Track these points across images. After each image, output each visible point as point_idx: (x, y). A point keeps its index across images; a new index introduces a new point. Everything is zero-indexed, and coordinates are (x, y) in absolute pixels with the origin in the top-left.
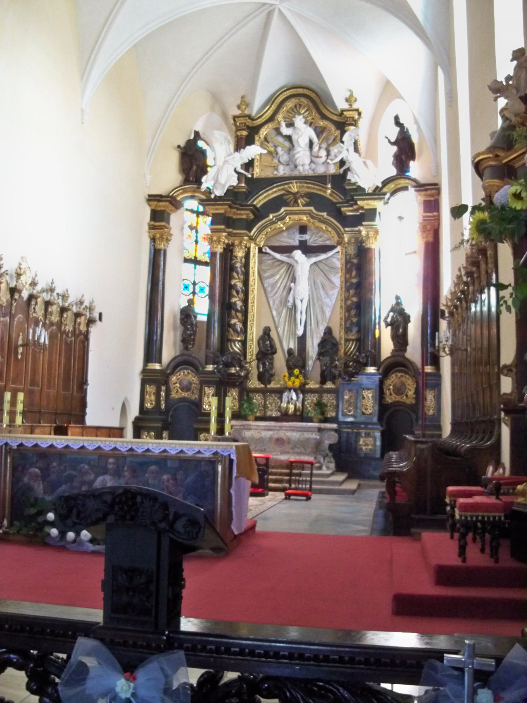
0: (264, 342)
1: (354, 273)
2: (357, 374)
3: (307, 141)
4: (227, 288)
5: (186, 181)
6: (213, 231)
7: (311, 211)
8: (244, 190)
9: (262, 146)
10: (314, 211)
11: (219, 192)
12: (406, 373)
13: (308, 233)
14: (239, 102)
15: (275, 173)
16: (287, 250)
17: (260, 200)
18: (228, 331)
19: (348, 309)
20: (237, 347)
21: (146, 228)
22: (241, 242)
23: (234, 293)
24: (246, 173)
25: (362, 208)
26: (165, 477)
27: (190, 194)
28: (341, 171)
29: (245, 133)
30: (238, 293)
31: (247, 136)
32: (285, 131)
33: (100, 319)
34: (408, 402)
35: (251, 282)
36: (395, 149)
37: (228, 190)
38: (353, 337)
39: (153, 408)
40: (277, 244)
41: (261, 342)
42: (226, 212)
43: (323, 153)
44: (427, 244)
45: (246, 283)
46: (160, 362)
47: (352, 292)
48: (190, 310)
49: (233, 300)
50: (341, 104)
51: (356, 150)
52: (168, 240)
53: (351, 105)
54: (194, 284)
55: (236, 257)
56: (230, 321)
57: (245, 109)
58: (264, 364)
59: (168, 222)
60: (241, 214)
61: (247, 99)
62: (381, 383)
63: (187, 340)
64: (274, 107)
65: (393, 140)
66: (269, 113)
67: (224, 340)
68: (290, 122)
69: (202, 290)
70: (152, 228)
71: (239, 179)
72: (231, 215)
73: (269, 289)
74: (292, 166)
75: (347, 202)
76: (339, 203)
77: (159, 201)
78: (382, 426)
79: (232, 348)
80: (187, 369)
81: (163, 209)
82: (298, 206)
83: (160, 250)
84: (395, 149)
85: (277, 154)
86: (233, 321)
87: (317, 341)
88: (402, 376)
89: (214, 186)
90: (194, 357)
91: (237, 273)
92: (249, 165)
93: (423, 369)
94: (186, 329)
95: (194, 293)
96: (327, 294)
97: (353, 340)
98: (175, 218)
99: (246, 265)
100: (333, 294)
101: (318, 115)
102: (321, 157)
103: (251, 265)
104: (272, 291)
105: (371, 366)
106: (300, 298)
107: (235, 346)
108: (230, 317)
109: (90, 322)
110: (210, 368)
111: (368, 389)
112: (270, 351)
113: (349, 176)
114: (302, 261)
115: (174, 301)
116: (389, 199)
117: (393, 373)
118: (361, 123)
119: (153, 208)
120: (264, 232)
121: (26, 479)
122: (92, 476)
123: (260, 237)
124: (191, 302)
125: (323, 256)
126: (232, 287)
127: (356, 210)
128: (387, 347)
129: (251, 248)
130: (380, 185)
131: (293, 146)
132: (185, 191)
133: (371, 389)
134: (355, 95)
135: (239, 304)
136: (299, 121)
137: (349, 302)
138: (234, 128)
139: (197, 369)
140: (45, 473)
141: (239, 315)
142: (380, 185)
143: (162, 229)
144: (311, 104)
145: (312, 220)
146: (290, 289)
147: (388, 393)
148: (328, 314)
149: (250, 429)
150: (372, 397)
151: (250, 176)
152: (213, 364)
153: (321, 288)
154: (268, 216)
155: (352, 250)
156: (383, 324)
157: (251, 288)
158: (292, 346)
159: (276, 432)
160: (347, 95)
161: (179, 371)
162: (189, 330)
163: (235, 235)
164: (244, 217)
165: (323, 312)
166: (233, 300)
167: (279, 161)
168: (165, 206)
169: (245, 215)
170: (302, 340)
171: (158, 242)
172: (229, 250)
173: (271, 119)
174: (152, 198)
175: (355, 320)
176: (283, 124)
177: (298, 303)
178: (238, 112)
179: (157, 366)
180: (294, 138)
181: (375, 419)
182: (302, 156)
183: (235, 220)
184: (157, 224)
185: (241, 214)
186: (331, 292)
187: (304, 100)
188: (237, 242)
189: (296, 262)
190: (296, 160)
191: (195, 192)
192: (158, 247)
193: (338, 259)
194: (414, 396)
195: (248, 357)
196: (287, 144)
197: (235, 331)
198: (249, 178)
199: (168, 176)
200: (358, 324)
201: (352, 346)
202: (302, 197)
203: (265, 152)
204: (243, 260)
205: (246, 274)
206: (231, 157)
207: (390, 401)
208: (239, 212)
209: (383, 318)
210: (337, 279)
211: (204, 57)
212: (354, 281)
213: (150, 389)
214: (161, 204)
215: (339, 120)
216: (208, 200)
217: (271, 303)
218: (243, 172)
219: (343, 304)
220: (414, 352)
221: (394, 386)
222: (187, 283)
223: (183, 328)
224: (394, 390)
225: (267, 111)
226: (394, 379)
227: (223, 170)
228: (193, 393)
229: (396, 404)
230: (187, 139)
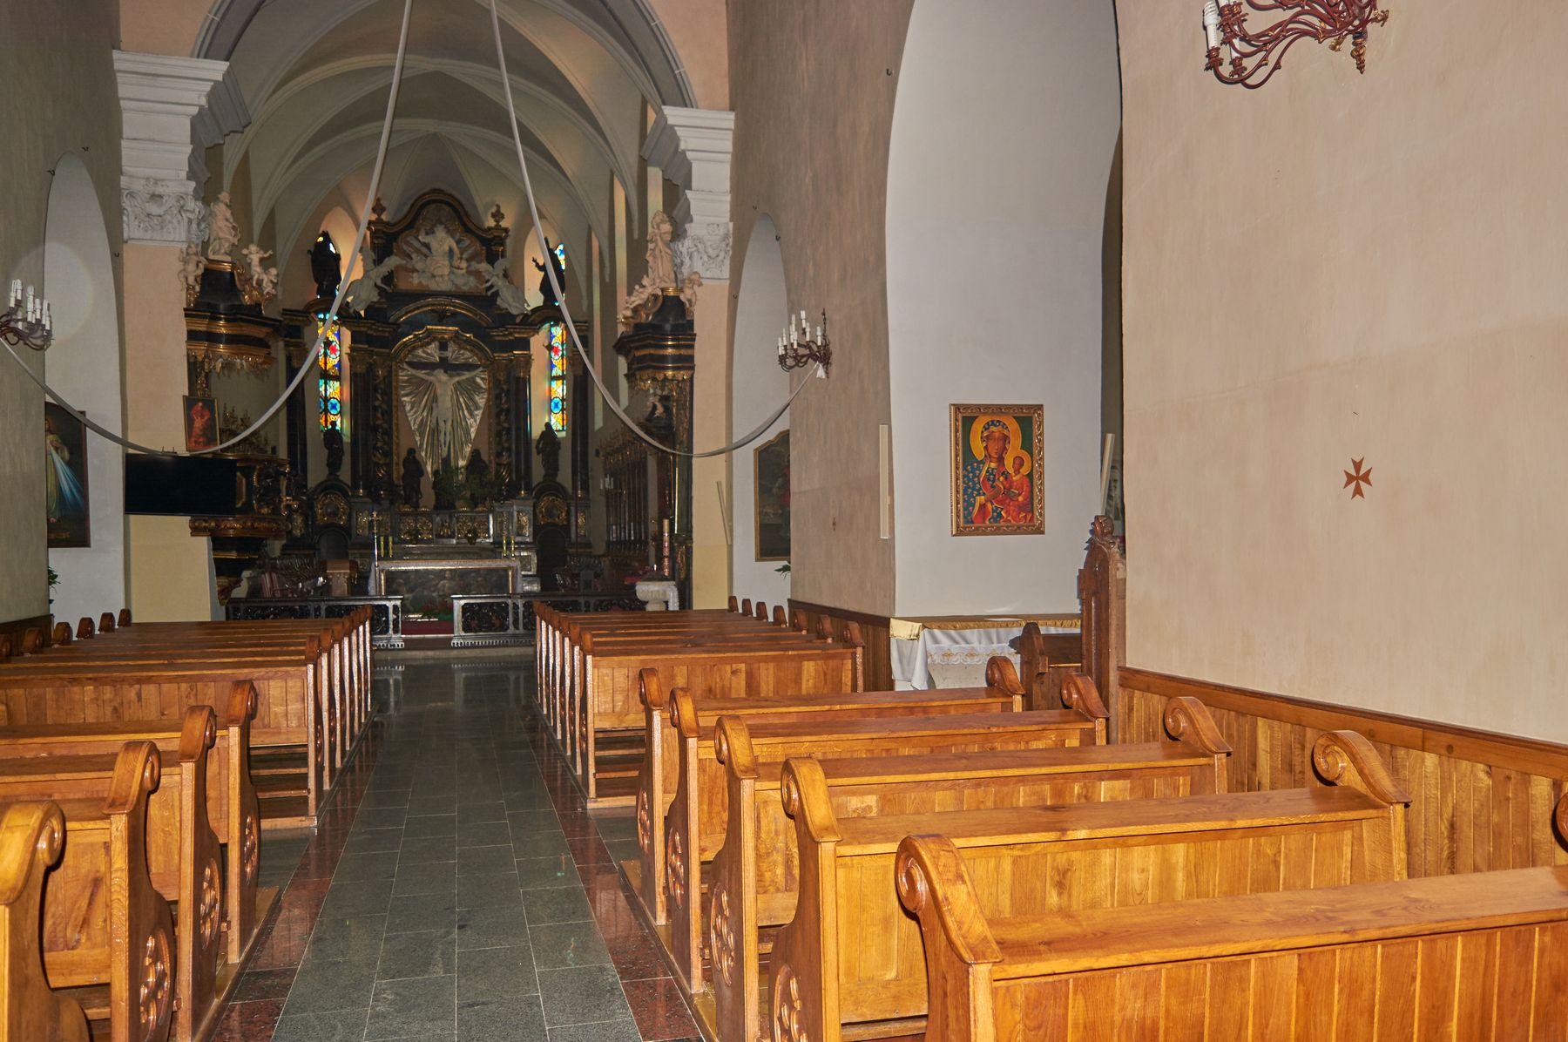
16: (431, 366)
43: (464, 265)
44: (575, 377)
45: (389, 402)
51: (505, 275)
63: (334, 463)
69: (334, 407)
92: (388, 279)
95: (326, 411)
96: (472, 415)
98: (307, 332)
113: (499, 301)
114: (444, 383)
115: (316, 425)
118: (508, 241)
125: (467, 375)
126: (376, 409)
136: (441, 233)
139: (345, 495)
160: (494, 210)
163: (378, 354)
165: (468, 433)
170: (446, 461)
172: (371, 368)
177: (441, 423)
178: (374, 217)
180: (434, 245)
187: (447, 209)
196: (424, 250)
210: (481, 400)
216: (346, 316)
220: (565, 477)
229: (547, 524)
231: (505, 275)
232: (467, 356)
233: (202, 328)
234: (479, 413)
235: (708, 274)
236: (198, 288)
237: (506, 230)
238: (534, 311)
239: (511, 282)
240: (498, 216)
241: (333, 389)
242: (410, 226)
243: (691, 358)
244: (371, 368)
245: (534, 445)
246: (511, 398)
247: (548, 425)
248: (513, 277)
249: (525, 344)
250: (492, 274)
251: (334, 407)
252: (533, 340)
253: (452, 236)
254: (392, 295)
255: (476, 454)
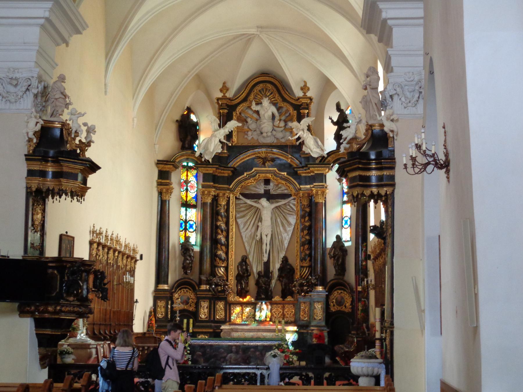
0: (242, 267)
1: (307, 219)
2: (311, 291)
3: (270, 114)
4: (215, 228)
5: (183, 148)
6: (203, 186)
7: (275, 171)
8: (226, 155)
9: (239, 120)
10: (277, 171)
11: (208, 157)
12: (345, 290)
13: (271, 184)
14: (221, 86)
15: (246, 136)
16: (257, 197)
17: (236, 162)
18: (215, 260)
19: (303, 244)
20: (221, 271)
21: (155, 184)
22: (224, 194)
23: (220, 231)
24: (228, 143)
25: (313, 172)
26: (257, 353)
27: (186, 157)
28: (298, 143)
29: (226, 111)
30: (222, 231)
31: (227, 113)
32: (254, 107)
33: (141, 258)
34: (347, 310)
35: (231, 223)
36: (336, 127)
37: (215, 156)
38: (306, 265)
39: (163, 318)
40: (247, 192)
41: (239, 267)
42: (214, 172)
43: (282, 124)
45: (227, 224)
46: (167, 284)
47: (306, 232)
48: (189, 245)
49: (219, 237)
50: (298, 93)
52: (171, 193)
53: (305, 93)
54: (186, 222)
55: (221, 205)
56: (217, 252)
57: (226, 92)
58: (241, 284)
59: (170, 180)
60: (224, 173)
61: (228, 85)
62: (327, 297)
64: (247, 91)
65: (335, 119)
66: (244, 95)
67: (214, 266)
68: (259, 102)
69: (191, 226)
70: (159, 184)
71: (222, 147)
72: (217, 174)
73: (241, 226)
74: (259, 132)
75: (303, 167)
76: (296, 168)
77: (166, 164)
78: (328, 328)
79: (219, 272)
80: (185, 288)
81: (168, 170)
82: (265, 167)
83: (165, 201)
84: (336, 127)
85: (247, 122)
86: (220, 252)
87: (278, 266)
88: (341, 293)
89: (205, 152)
90: (192, 280)
91: (222, 217)
92: (229, 136)
93: (357, 288)
94: (186, 259)
95: (186, 229)
96: (285, 230)
97: (307, 267)
99: (227, 211)
100: (290, 230)
101: (280, 98)
102: (281, 127)
103: (231, 210)
104: (244, 227)
105: (320, 286)
106: (265, 233)
107: (221, 270)
108: (216, 248)
109: (136, 261)
110: (204, 287)
111: (318, 302)
112: (246, 275)
113: (304, 149)
116: (332, 167)
117: (335, 291)
118: (313, 106)
119: (160, 169)
120: (240, 186)
121: (195, 357)
122: (226, 354)
123: (237, 189)
124: (187, 238)
125: (282, 202)
126: (217, 227)
127: (309, 173)
128: (331, 272)
129: (231, 198)
130: (326, 156)
131: (260, 117)
132: (182, 156)
133: (320, 302)
134: (308, 85)
135: (223, 240)
136: (266, 102)
137: (304, 240)
138: (217, 106)
139: (194, 289)
140: (204, 354)
141: (224, 248)
142: (326, 156)
143: (168, 185)
144: (275, 90)
145: (275, 178)
146: (258, 226)
147: (332, 304)
148: (286, 245)
149: (237, 332)
150: (321, 307)
151: (230, 145)
152: (206, 284)
153: (280, 225)
154: (244, 174)
155: (305, 202)
156: (328, 256)
157: (230, 228)
158: (259, 269)
159: (255, 333)
160: (302, 85)
161: (180, 289)
162: (188, 260)
164: (226, 175)
166: (219, 237)
167: (248, 128)
168: (169, 168)
169: (227, 173)
170: (267, 265)
171: (164, 194)
172: (215, 199)
173: (245, 100)
174: (159, 163)
175: (308, 252)
176: (254, 103)
177: (264, 237)
178: (220, 95)
179: (166, 287)
180: (262, 112)
181: (323, 324)
182: (267, 126)
183: (219, 177)
184: (163, 181)
185: (224, 173)
186: (288, 229)
187: (269, 85)
188: (221, 194)
189: (263, 206)
190: (262, 128)
191: (189, 155)
192: (164, 198)
193: (294, 205)
194: (351, 306)
195: (230, 278)
196: (255, 116)
197: (220, 259)
198: (229, 146)
199: (168, 143)
200: (310, 255)
201: (306, 271)
202: (269, 161)
203: (240, 125)
204: (226, 207)
205: (228, 217)
206: (218, 132)
207: (334, 310)
208: (222, 171)
209: (328, 252)
210: (293, 220)
211: (202, 61)
212: (307, 224)
213: (161, 304)
214: (166, 166)
215: (296, 103)
216: (200, 163)
217: (244, 236)
218: (225, 141)
219: (299, 240)
221: (336, 300)
222: (181, 221)
223: (183, 258)
224: (336, 302)
225: (242, 94)
226: (336, 294)
227: (210, 138)
228: (190, 305)
230: (181, 113)
231: (309, 129)
232: (283, 190)
233: (37, 167)
234: (290, 229)
235: (406, 111)
236: (35, 140)
237: (311, 99)
238: (329, 154)
239: (311, 134)
240: (305, 88)
241: (193, 215)
242: (245, 100)
243: (392, 178)
244: (215, 199)
245: (328, 252)
246: (312, 215)
247: (339, 238)
248: (316, 131)
249: (322, 178)
250: (300, 129)
251: (191, 226)
252: (328, 175)
253: (275, 104)
254: (231, 149)
255: (285, 260)
